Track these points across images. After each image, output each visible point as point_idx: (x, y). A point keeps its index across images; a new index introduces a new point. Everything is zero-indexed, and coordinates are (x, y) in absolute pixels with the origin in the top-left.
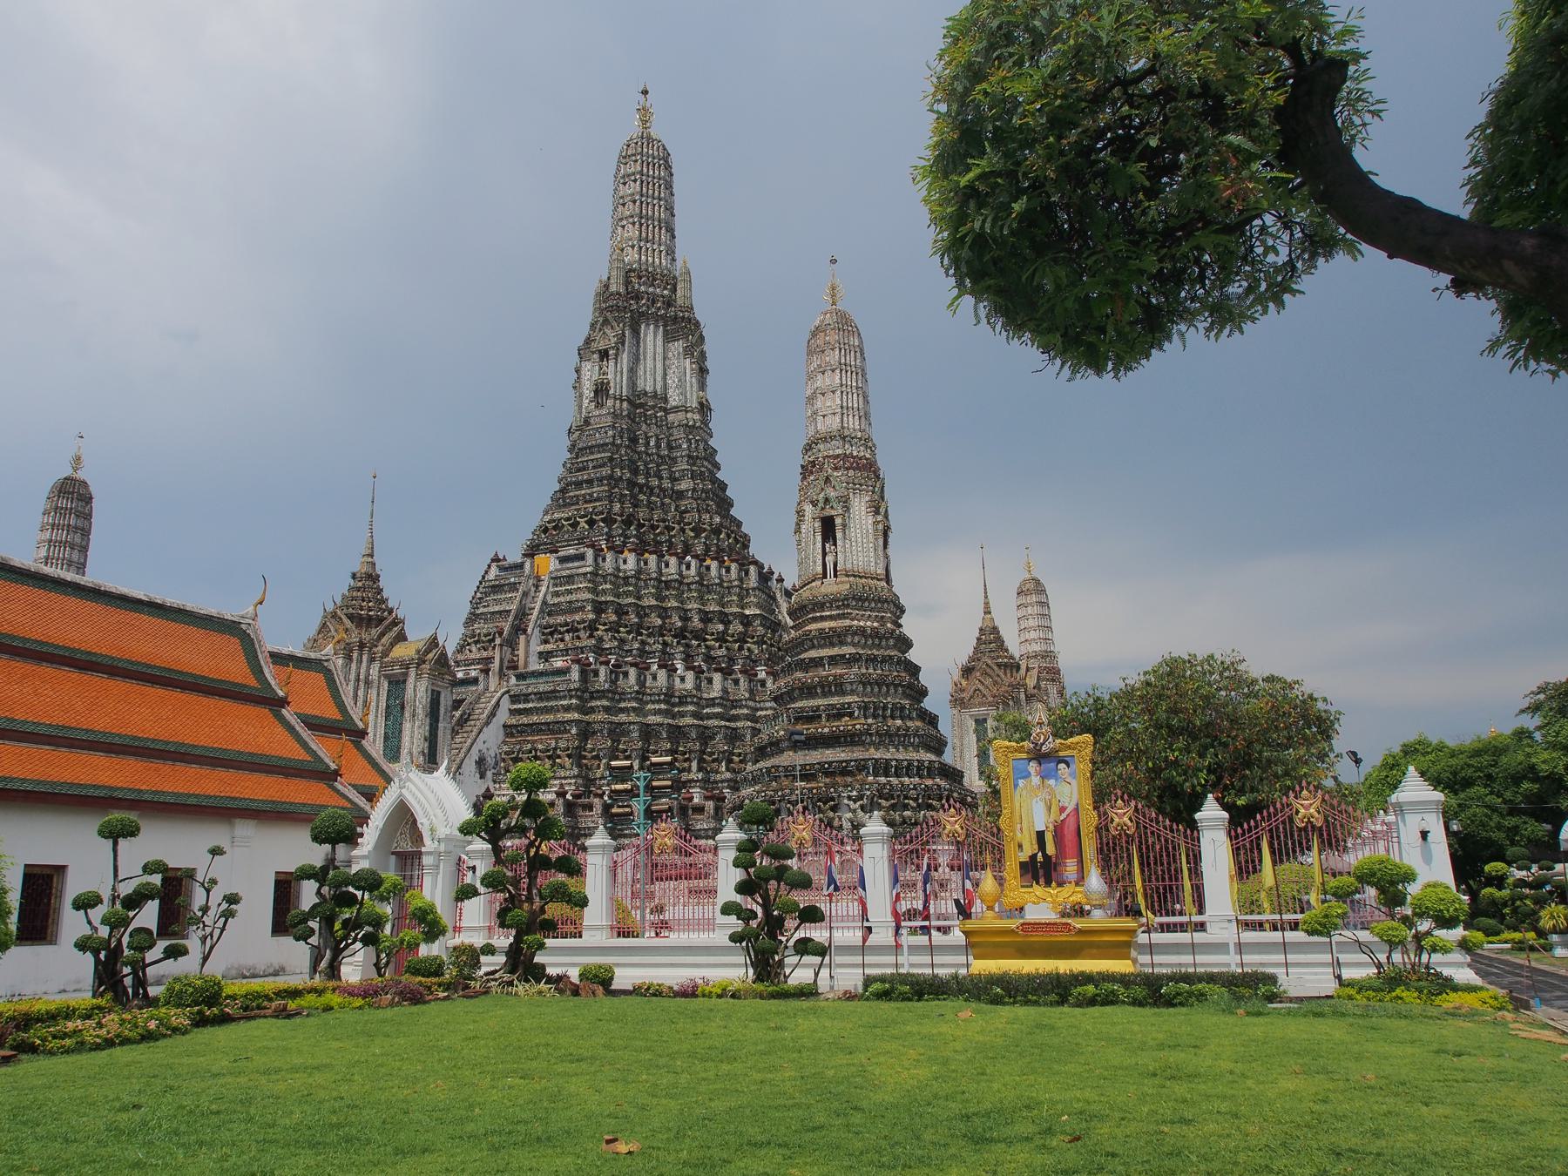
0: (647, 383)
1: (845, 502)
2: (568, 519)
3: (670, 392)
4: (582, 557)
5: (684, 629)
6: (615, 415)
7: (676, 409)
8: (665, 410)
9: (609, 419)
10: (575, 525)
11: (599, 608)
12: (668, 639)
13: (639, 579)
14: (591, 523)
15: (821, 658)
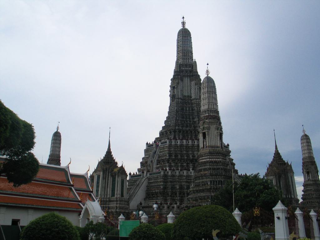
0: (186, 94)
1: (209, 129)
2: (165, 132)
3: (192, 95)
4: (166, 142)
5: (193, 159)
6: (177, 103)
7: (194, 99)
8: (191, 100)
9: (176, 104)
10: (167, 133)
11: (170, 155)
12: (189, 162)
13: (181, 147)
14: (171, 132)
15: (201, 169)
